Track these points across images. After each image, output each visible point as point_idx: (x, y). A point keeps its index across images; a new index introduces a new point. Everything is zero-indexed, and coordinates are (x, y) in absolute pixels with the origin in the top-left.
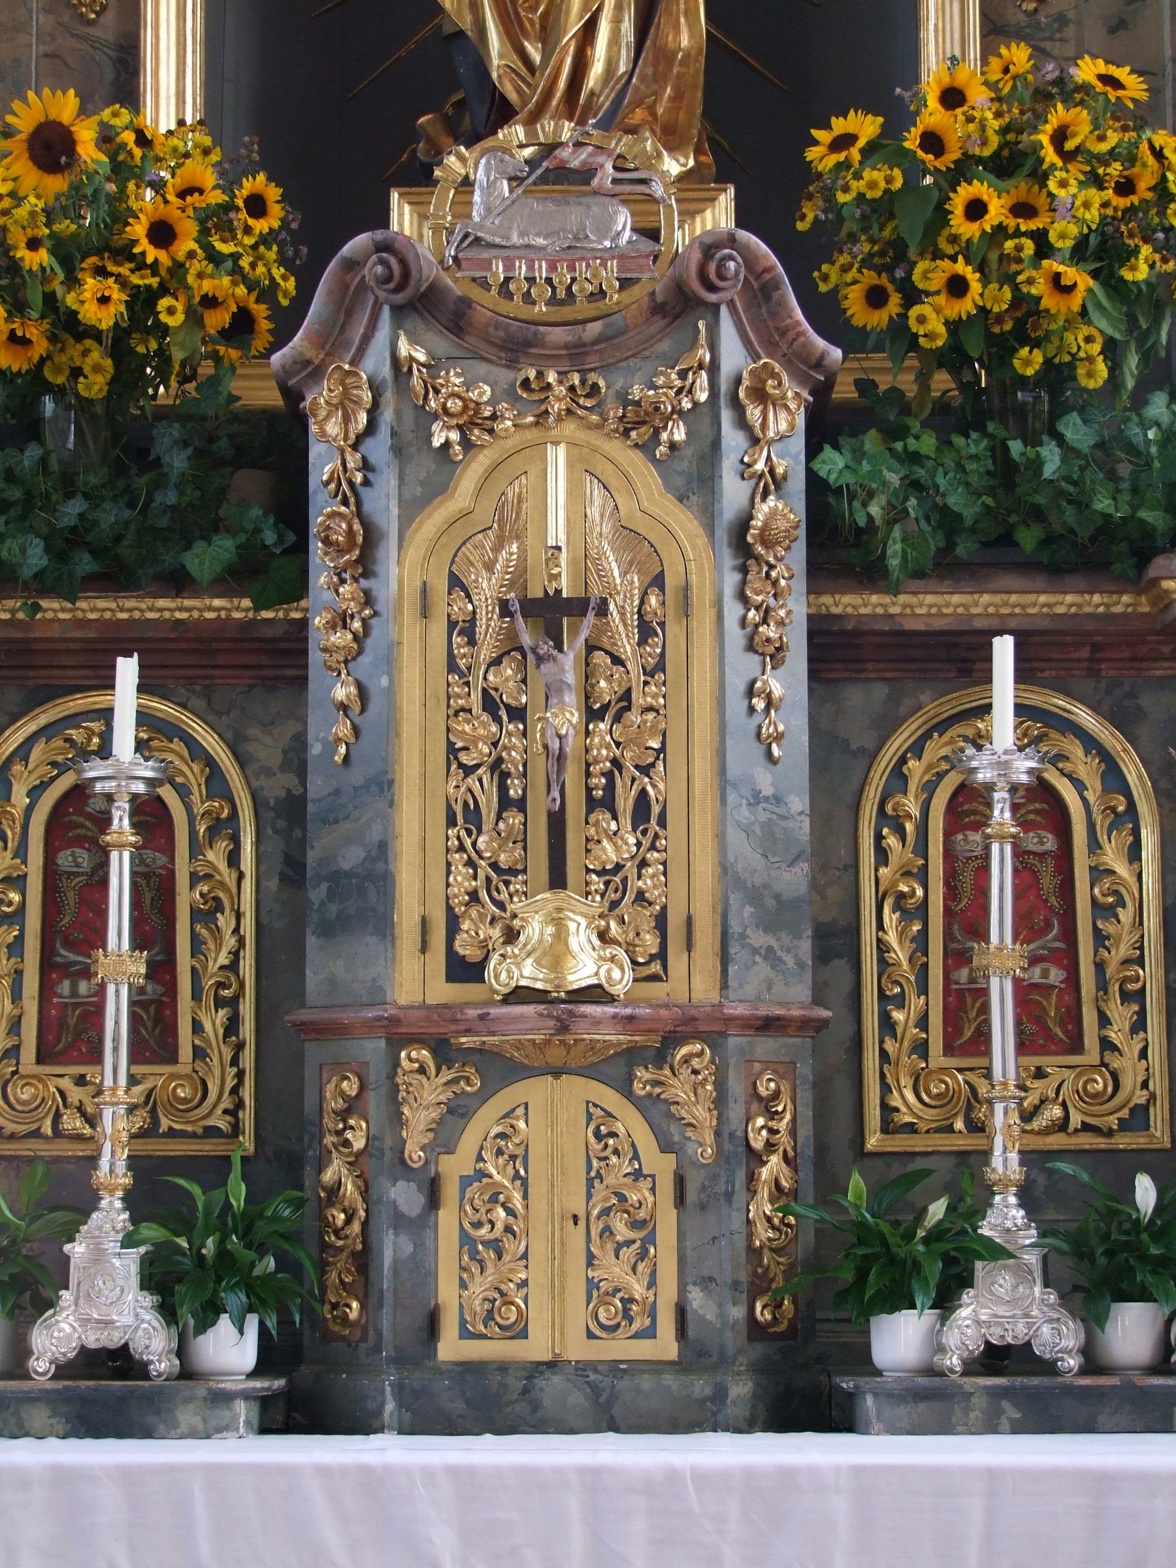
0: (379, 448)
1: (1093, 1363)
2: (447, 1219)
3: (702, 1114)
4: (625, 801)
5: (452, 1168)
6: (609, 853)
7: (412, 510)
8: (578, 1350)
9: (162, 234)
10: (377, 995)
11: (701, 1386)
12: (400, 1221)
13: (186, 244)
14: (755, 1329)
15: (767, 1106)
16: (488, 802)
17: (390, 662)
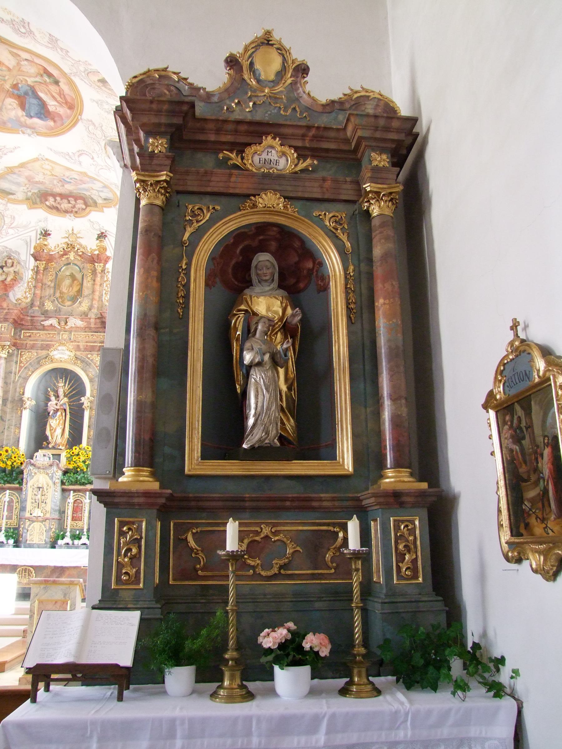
0: (28, 475)
1: (73, 544)
2: (29, 533)
3: (48, 525)
4: (44, 502)
5: (29, 529)
6: (43, 506)
7: (30, 480)
8: (37, 542)
9: (15, 457)
10: (24, 516)
11: (46, 545)
12: (25, 533)
13: (17, 458)
14: (50, 541)
15: (53, 525)
16: (34, 502)
17: (27, 491)
